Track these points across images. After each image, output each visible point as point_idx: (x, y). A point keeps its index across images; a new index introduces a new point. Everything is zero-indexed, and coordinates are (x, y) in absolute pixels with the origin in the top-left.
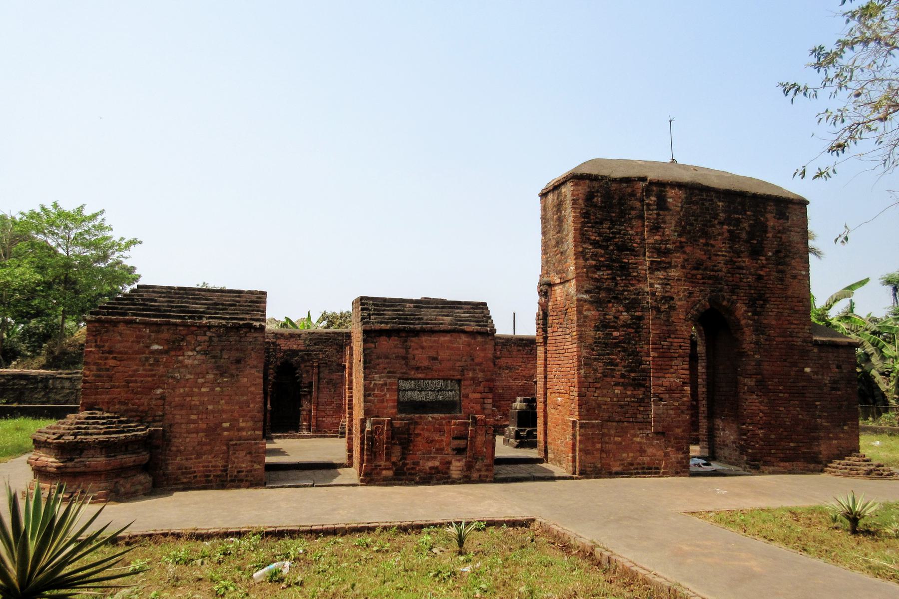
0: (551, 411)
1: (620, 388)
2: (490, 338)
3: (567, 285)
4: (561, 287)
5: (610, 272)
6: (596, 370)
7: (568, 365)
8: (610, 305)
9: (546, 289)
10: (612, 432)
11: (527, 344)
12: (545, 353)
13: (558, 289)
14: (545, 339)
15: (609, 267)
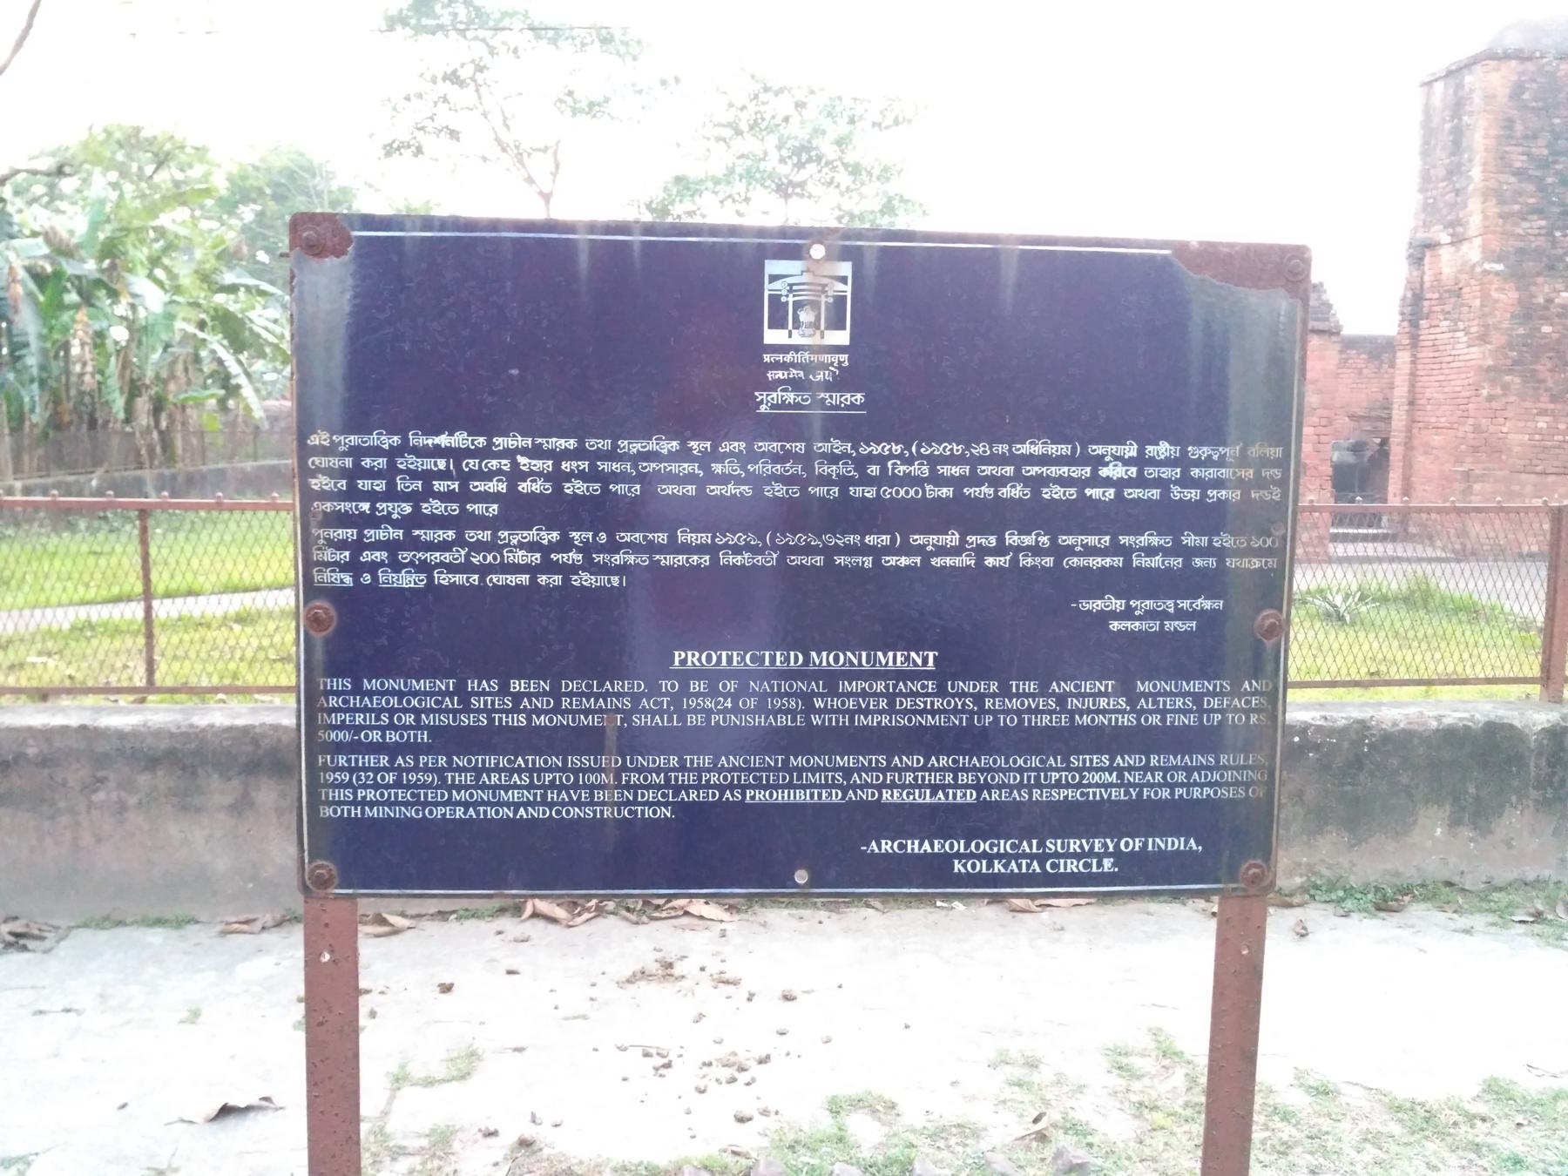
0: (1422, 461)
1: (1547, 419)
2: (1334, 338)
3: (1465, 247)
4: (1452, 249)
5: (1543, 223)
6: (1506, 387)
7: (1459, 382)
8: (1540, 280)
9: (1421, 251)
10: (1529, 489)
11: (1379, 350)
12: (1413, 362)
13: (1446, 254)
14: (1415, 341)
15: (1539, 212)
